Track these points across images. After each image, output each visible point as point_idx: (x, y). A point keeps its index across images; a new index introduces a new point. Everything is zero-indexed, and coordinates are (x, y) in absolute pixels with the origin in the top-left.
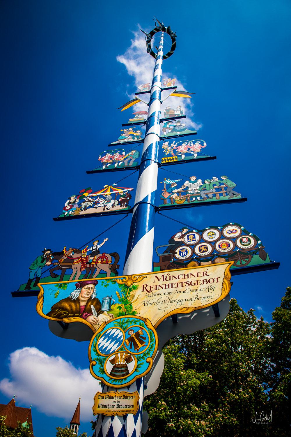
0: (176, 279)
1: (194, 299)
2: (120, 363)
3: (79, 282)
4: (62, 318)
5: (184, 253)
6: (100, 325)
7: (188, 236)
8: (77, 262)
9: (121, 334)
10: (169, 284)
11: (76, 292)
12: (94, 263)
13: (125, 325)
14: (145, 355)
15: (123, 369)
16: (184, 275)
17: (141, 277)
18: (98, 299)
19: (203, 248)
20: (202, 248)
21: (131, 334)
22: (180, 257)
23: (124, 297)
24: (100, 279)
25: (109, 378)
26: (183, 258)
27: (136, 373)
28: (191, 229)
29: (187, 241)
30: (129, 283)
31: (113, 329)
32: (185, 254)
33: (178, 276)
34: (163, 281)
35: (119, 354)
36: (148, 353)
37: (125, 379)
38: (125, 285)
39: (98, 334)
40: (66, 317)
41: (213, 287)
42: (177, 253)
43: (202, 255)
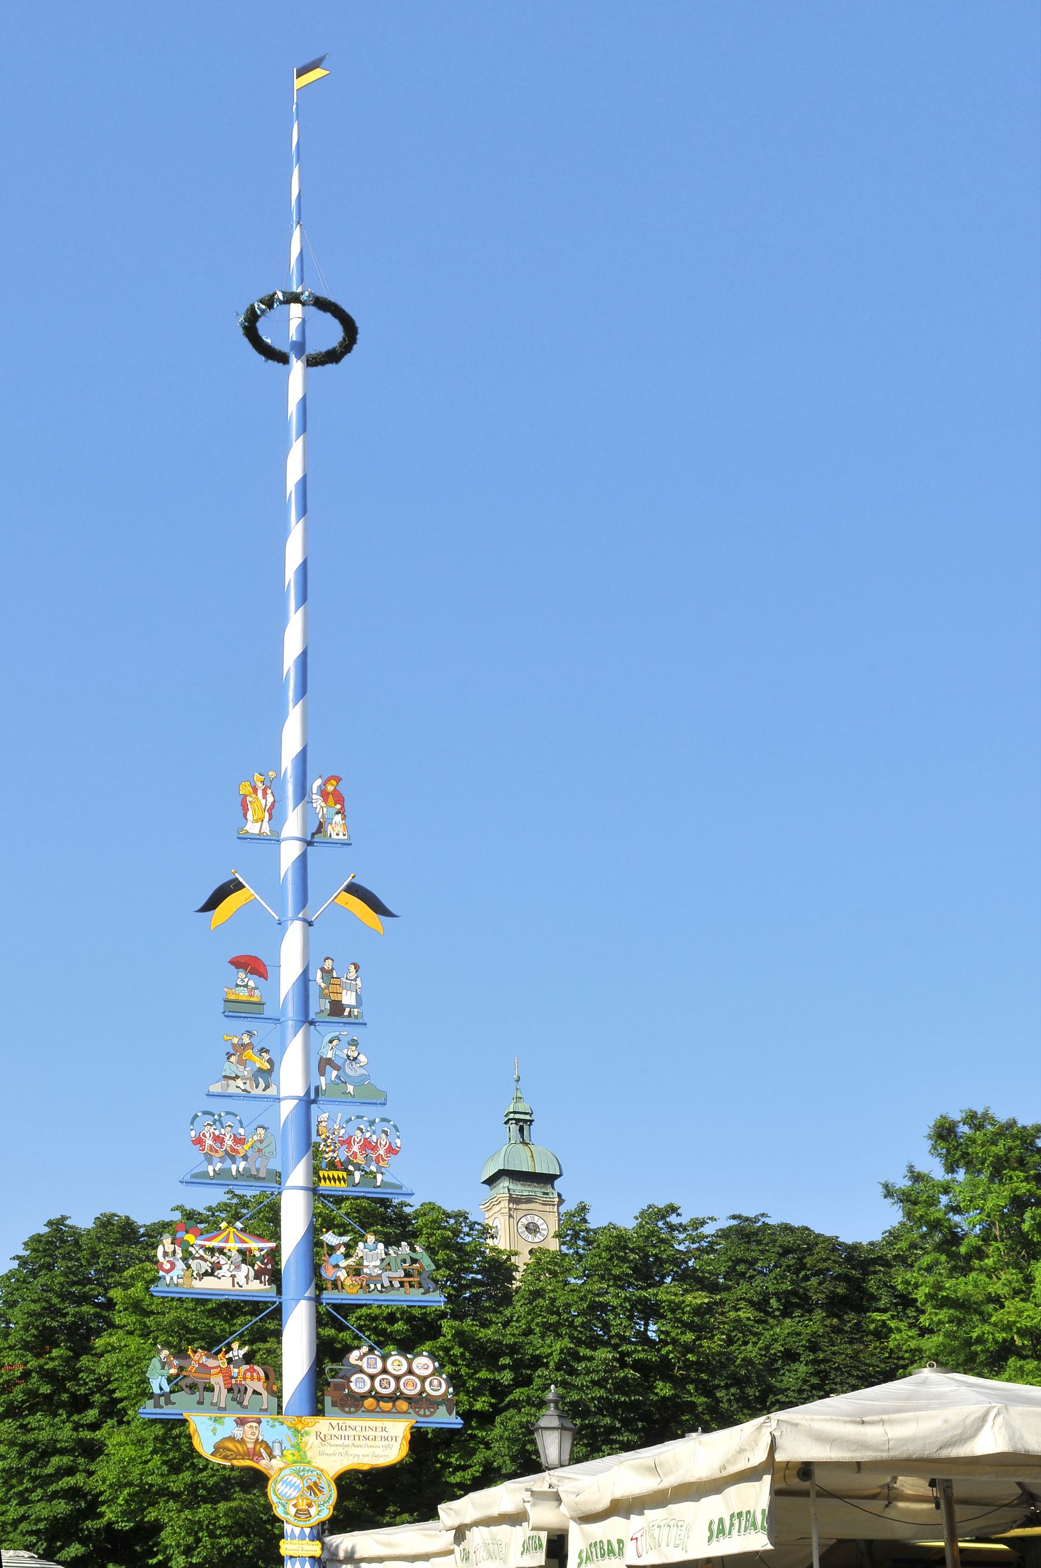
24: (265, 1418)
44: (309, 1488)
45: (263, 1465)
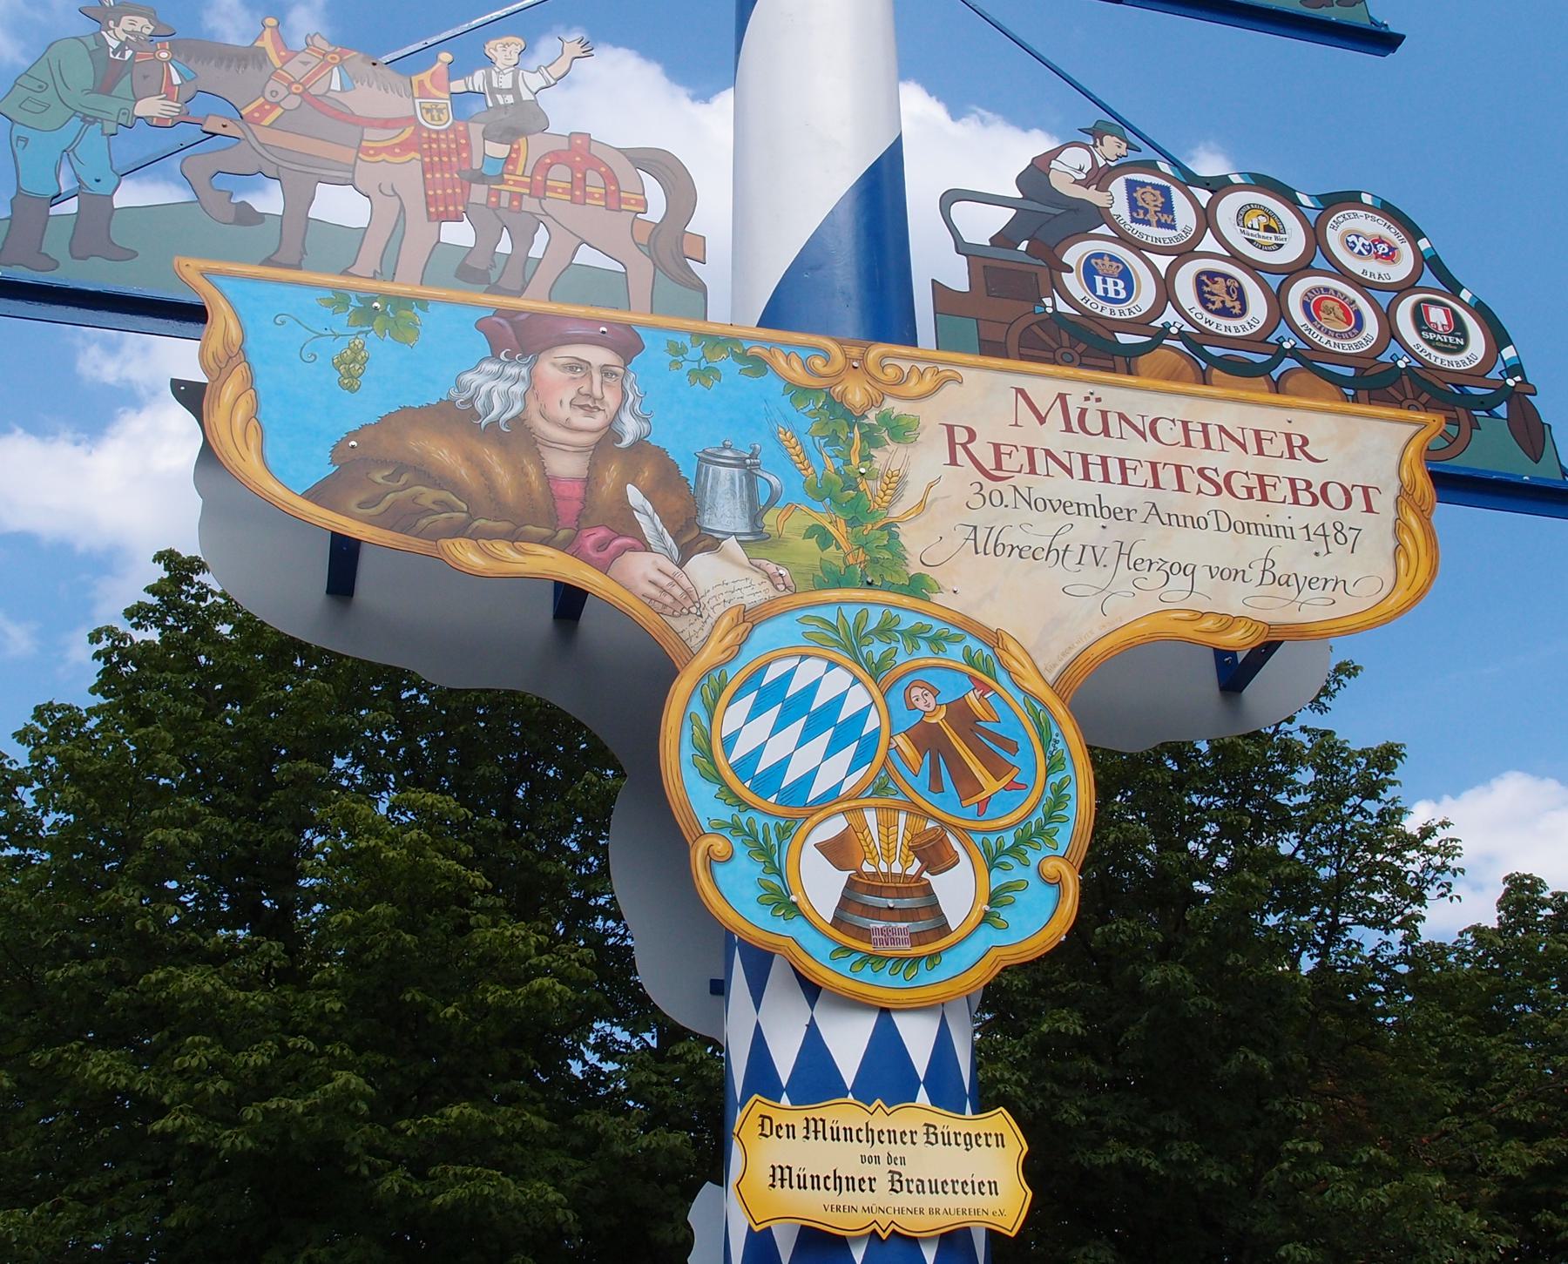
0: (1143, 436)
1: (1254, 575)
2: (884, 868)
3: (499, 312)
4: (434, 535)
5: (1116, 284)
6: (710, 621)
7: (1132, 186)
8: (389, 150)
9: (857, 700)
10: (1104, 460)
11: (498, 376)
12: (516, 183)
13: (877, 649)
14: (1025, 839)
15: (906, 903)
16: (1185, 424)
17: (928, 376)
18: (661, 453)
19: (1219, 287)
20: (1215, 288)
21: (921, 705)
22: (1093, 299)
23: (837, 472)
25: (832, 947)
26: (1106, 313)
27: (987, 937)
28: (1148, 154)
29: (1127, 219)
30: (856, 395)
31: (804, 657)
32: (1117, 293)
33: (1148, 421)
34: (1069, 429)
35: (871, 817)
36: (1041, 831)
37: (933, 957)
38: (828, 394)
39: (707, 674)
40: (459, 531)
41: (1351, 535)
42: (1069, 269)
43: (1213, 328)
44: (927, 739)
45: (637, 579)
